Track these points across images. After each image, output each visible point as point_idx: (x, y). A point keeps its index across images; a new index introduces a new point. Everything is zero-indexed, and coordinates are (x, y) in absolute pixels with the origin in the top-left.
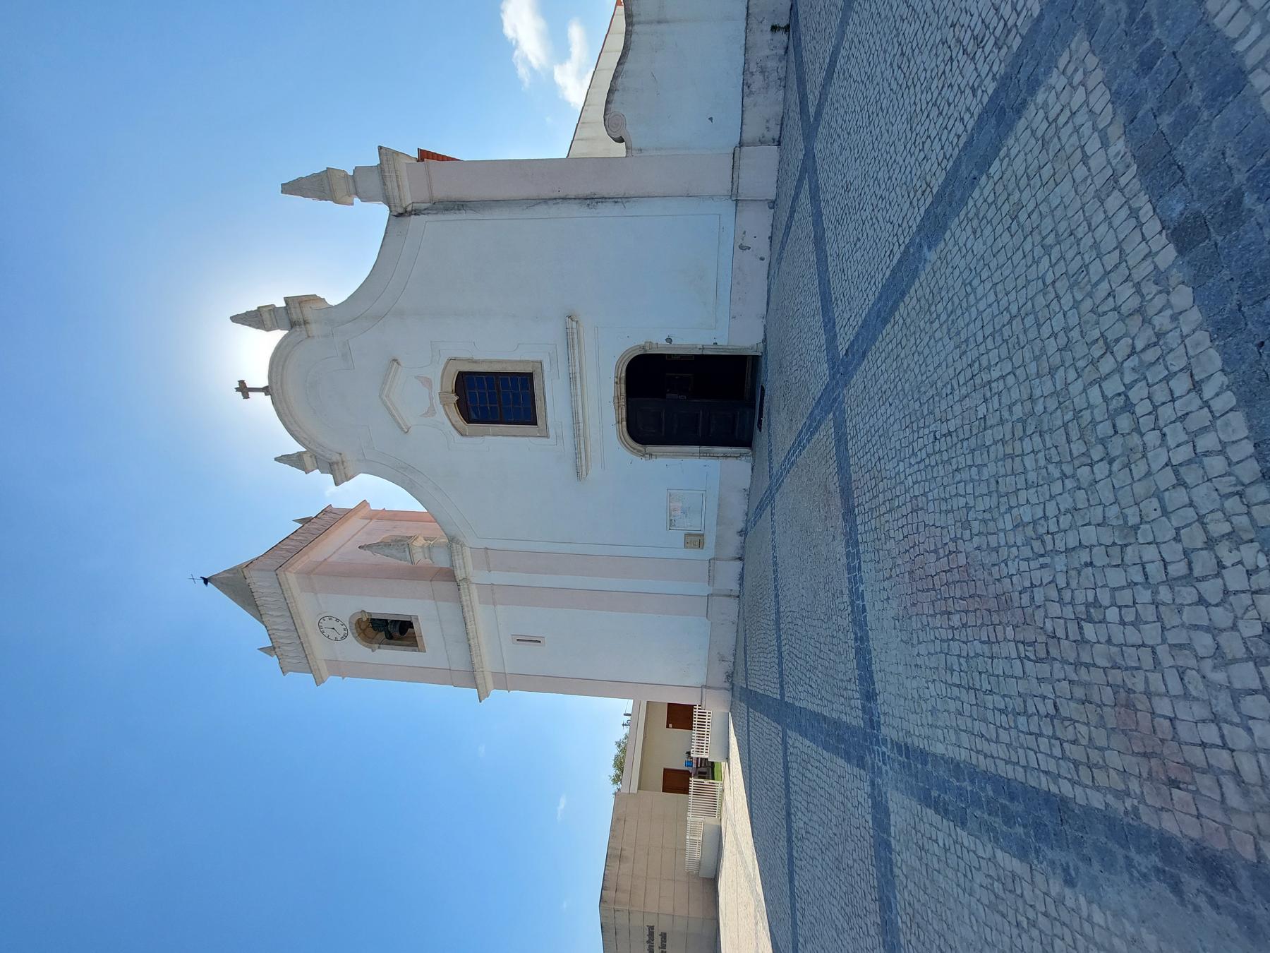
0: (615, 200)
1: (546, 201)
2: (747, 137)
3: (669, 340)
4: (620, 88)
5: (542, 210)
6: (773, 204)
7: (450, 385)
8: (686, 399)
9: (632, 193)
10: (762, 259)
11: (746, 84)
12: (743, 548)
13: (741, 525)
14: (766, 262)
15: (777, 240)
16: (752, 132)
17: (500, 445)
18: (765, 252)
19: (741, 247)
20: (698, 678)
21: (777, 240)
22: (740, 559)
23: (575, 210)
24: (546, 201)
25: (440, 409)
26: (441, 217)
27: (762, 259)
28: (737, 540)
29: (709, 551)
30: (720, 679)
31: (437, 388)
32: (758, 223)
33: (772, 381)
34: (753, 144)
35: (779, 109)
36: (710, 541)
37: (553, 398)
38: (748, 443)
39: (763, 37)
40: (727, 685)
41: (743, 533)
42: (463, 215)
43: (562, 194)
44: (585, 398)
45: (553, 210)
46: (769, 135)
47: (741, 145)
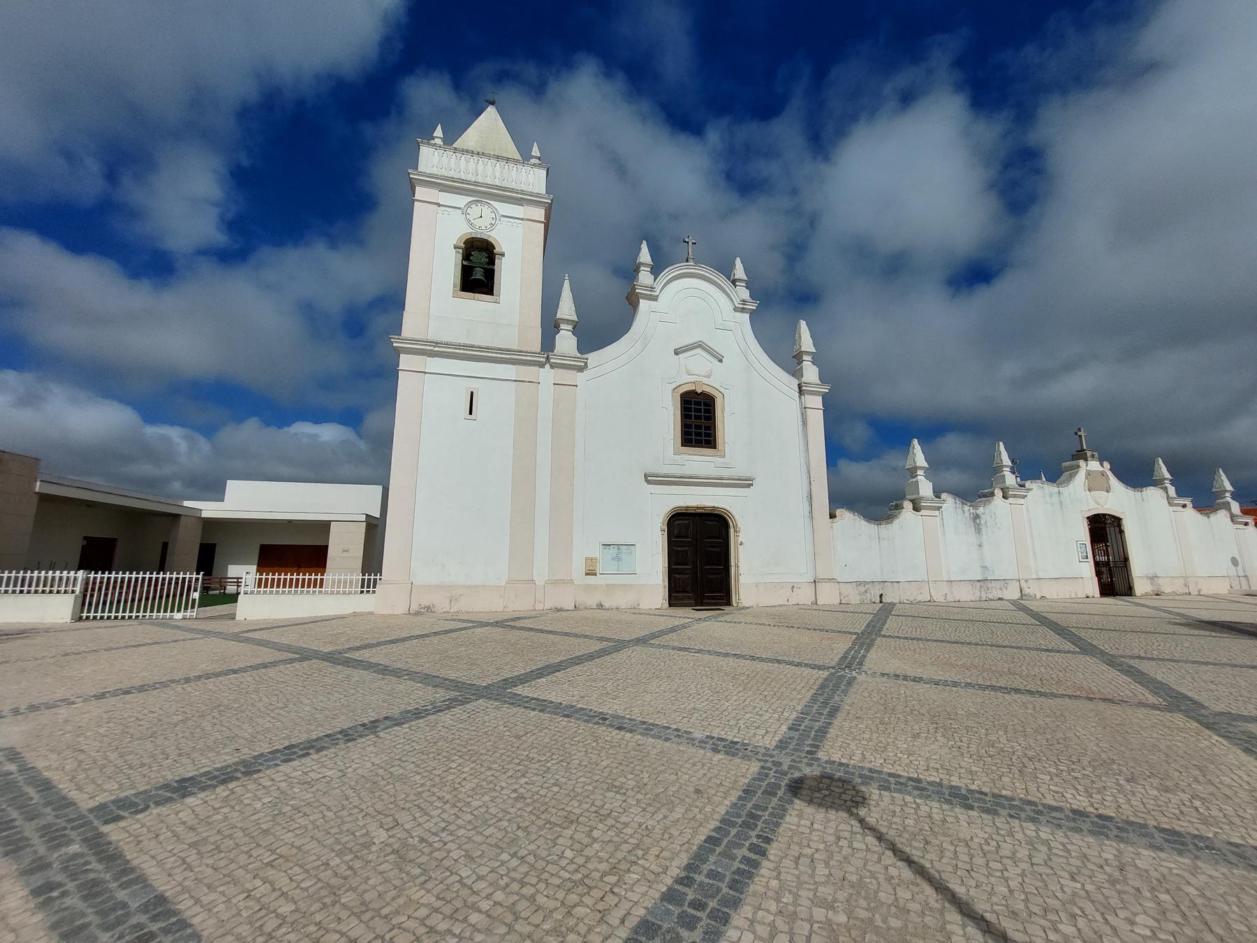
0: (811, 512)
5: (804, 468)
8: (700, 557)
11: (859, 583)
13: (607, 604)
17: (669, 420)
18: (792, 602)
20: (424, 575)
23: (806, 489)
25: (692, 379)
28: (592, 602)
30: (419, 601)
31: (705, 381)
32: (804, 596)
33: (727, 613)
36: (591, 580)
37: (698, 461)
39: (875, 593)
40: (414, 608)
41: (600, 606)
44: (701, 483)
45: (805, 476)
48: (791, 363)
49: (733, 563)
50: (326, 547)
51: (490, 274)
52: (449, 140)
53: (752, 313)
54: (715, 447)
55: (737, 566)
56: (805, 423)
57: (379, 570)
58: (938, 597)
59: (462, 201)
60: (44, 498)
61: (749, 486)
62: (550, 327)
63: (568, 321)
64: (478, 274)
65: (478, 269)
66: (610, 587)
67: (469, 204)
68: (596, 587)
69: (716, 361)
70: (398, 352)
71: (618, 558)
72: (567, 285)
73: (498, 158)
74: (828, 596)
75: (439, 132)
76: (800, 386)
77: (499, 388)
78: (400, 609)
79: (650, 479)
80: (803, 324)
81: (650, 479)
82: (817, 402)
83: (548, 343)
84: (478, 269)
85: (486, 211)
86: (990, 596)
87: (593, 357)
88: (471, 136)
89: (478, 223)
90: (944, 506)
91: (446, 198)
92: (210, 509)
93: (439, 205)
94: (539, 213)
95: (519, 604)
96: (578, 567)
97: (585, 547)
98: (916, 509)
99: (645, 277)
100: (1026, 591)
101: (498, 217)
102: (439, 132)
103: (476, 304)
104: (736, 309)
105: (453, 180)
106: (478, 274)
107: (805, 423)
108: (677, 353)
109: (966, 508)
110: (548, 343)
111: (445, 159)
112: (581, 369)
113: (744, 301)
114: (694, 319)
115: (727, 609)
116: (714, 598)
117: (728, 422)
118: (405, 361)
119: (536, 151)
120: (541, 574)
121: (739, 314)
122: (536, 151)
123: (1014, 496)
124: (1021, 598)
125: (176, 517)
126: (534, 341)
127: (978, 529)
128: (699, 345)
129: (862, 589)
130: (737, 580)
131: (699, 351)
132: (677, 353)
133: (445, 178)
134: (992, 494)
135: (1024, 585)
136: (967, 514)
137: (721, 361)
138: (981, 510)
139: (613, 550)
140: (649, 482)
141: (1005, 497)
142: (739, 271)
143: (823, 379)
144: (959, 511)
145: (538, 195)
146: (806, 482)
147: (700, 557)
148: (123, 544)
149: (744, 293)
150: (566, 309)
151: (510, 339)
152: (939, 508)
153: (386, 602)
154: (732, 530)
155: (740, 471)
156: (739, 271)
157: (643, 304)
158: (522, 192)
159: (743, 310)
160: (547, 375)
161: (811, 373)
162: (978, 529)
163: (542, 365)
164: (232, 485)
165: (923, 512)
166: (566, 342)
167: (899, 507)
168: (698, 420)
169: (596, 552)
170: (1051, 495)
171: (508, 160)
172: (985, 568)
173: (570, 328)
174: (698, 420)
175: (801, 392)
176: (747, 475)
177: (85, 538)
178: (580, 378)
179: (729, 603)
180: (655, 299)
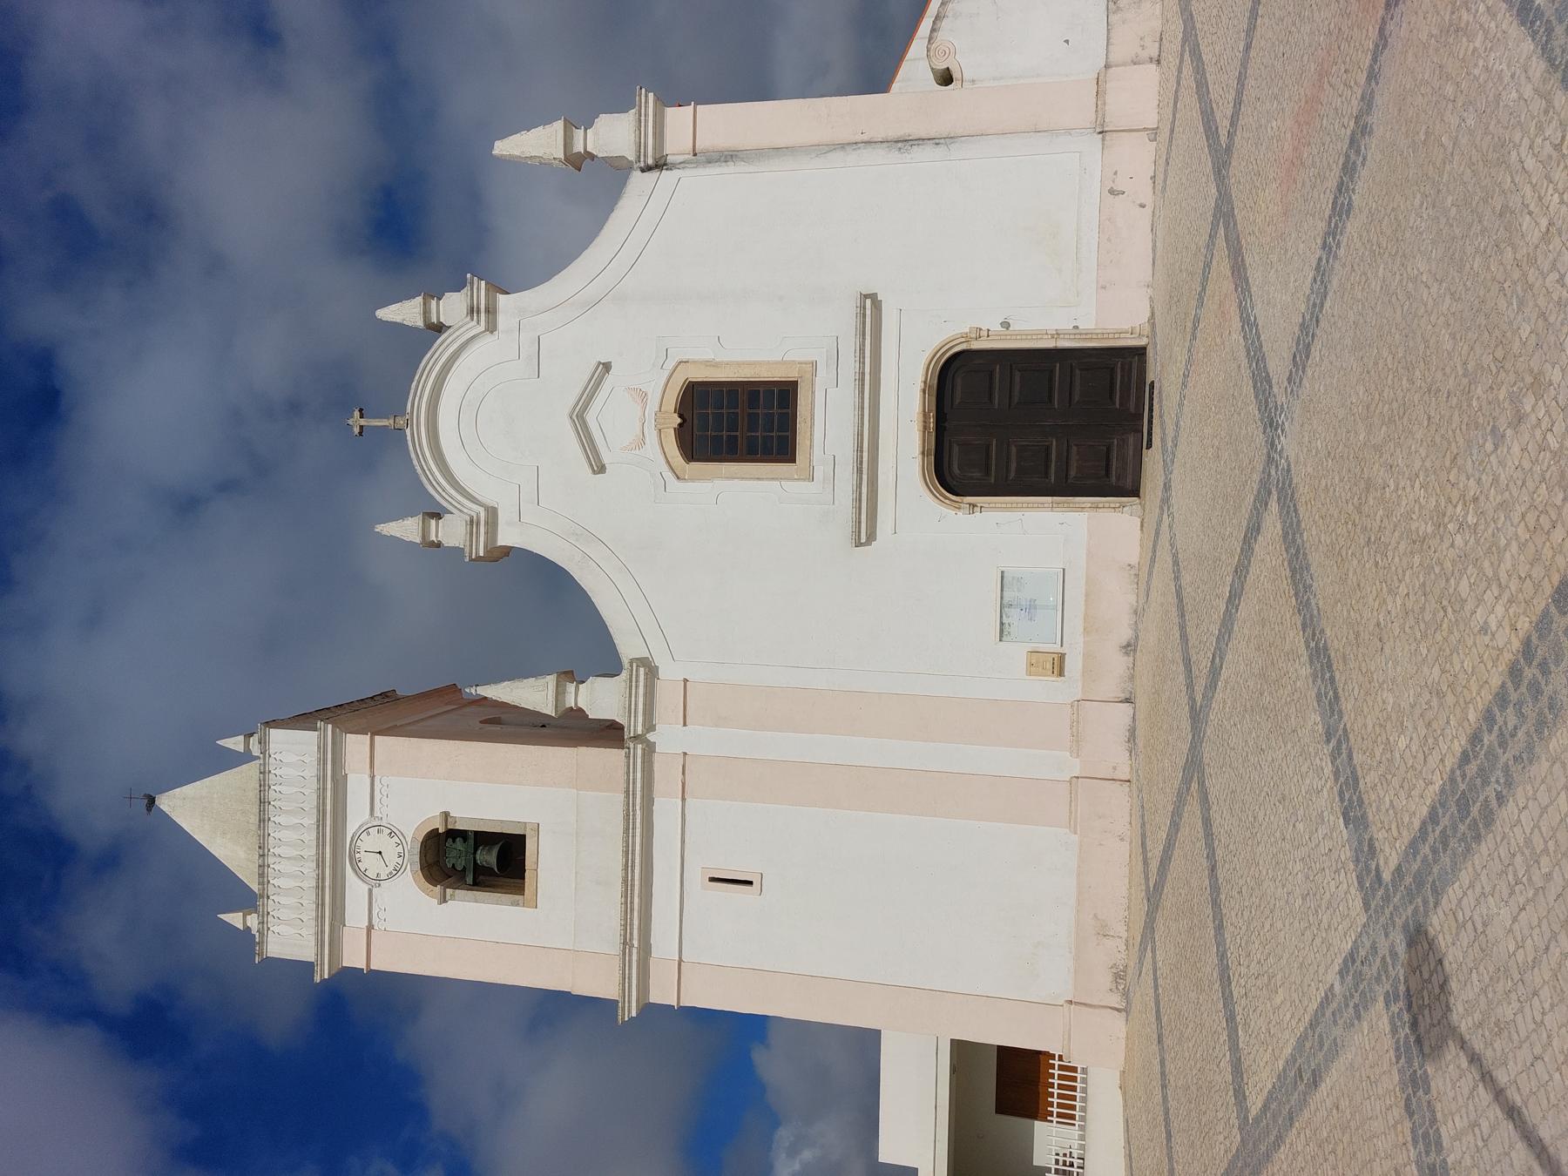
0: (935, 141)
1: (843, 146)
2: (1113, 58)
3: (1006, 325)
4: (950, 14)
5: (838, 156)
6: (1154, 133)
7: (671, 402)
8: (1032, 421)
9: (960, 132)
10: (1143, 206)
12: (1132, 678)
13: (1125, 634)
14: (1149, 210)
15: (1159, 180)
17: (739, 489)
18: (1146, 194)
19: (1112, 192)
20: (1056, 981)
21: (1159, 180)
22: (1127, 701)
24: (843, 146)
26: (700, 171)
27: (1143, 206)
28: (1120, 663)
30: (1101, 989)
31: (653, 405)
32: (1137, 160)
33: (1164, 372)
34: (1124, 64)
35: (1157, 24)
36: (1073, 665)
37: (826, 423)
38: (1134, 492)
40: (1116, 1000)
41: (1129, 648)
42: (730, 168)
43: (865, 138)
46: (1145, 55)
47: (1107, 66)
48: (596, 184)
49: (1050, 344)
50: (1000, 1048)
51: (483, 839)
52: (249, 900)
53: (498, 288)
54: (794, 384)
55: (1057, 335)
59: (355, 890)
61: (877, 305)
63: (560, 693)
64: (489, 858)
65: (480, 860)
66: (1091, 626)
67: (361, 874)
68: (1087, 656)
69: (609, 380)
70: (650, 1011)
71: (1031, 608)
73: (263, 821)
74: (1140, 95)
75: (235, 919)
76: (647, 169)
77: (701, 829)
79: (865, 532)
80: (503, 148)
81: (865, 532)
82: (678, 119)
83: (609, 733)
84: (480, 860)
87: (628, 648)
88: (231, 851)
91: (355, 915)
93: (370, 927)
94: (356, 744)
95: (1118, 806)
96: (1046, 689)
99: (451, 532)
102: (235, 919)
103: (543, 860)
104: (492, 328)
105: (320, 905)
108: (601, 469)
110: (609, 733)
111: (284, 914)
112: (652, 672)
113: (472, 311)
114: (524, 415)
115: (1150, 353)
117: (742, 352)
118: (663, 993)
119: (235, 743)
120: (1059, 764)
121: (502, 320)
122: (235, 743)
126: (609, 758)
128: (579, 418)
130: (1088, 335)
131: (590, 417)
132: (601, 469)
133: (320, 918)
137: (607, 367)
139: (1013, 616)
140: (871, 537)
142: (406, 312)
143: (621, 104)
145: (322, 748)
146: (867, 154)
147: (1032, 421)
149: (452, 307)
151: (607, 807)
154: (976, 345)
155: (843, 322)
156: (406, 312)
157: (505, 538)
158: (322, 779)
159: (491, 311)
160: (668, 738)
161: (612, 135)
163: (650, 748)
166: (600, 698)
168: (737, 422)
169: (1016, 653)
171: (263, 786)
173: (571, 687)
174: (737, 422)
175: (660, 165)
178: (669, 673)
179: (1140, 353)
180: (492, 513)
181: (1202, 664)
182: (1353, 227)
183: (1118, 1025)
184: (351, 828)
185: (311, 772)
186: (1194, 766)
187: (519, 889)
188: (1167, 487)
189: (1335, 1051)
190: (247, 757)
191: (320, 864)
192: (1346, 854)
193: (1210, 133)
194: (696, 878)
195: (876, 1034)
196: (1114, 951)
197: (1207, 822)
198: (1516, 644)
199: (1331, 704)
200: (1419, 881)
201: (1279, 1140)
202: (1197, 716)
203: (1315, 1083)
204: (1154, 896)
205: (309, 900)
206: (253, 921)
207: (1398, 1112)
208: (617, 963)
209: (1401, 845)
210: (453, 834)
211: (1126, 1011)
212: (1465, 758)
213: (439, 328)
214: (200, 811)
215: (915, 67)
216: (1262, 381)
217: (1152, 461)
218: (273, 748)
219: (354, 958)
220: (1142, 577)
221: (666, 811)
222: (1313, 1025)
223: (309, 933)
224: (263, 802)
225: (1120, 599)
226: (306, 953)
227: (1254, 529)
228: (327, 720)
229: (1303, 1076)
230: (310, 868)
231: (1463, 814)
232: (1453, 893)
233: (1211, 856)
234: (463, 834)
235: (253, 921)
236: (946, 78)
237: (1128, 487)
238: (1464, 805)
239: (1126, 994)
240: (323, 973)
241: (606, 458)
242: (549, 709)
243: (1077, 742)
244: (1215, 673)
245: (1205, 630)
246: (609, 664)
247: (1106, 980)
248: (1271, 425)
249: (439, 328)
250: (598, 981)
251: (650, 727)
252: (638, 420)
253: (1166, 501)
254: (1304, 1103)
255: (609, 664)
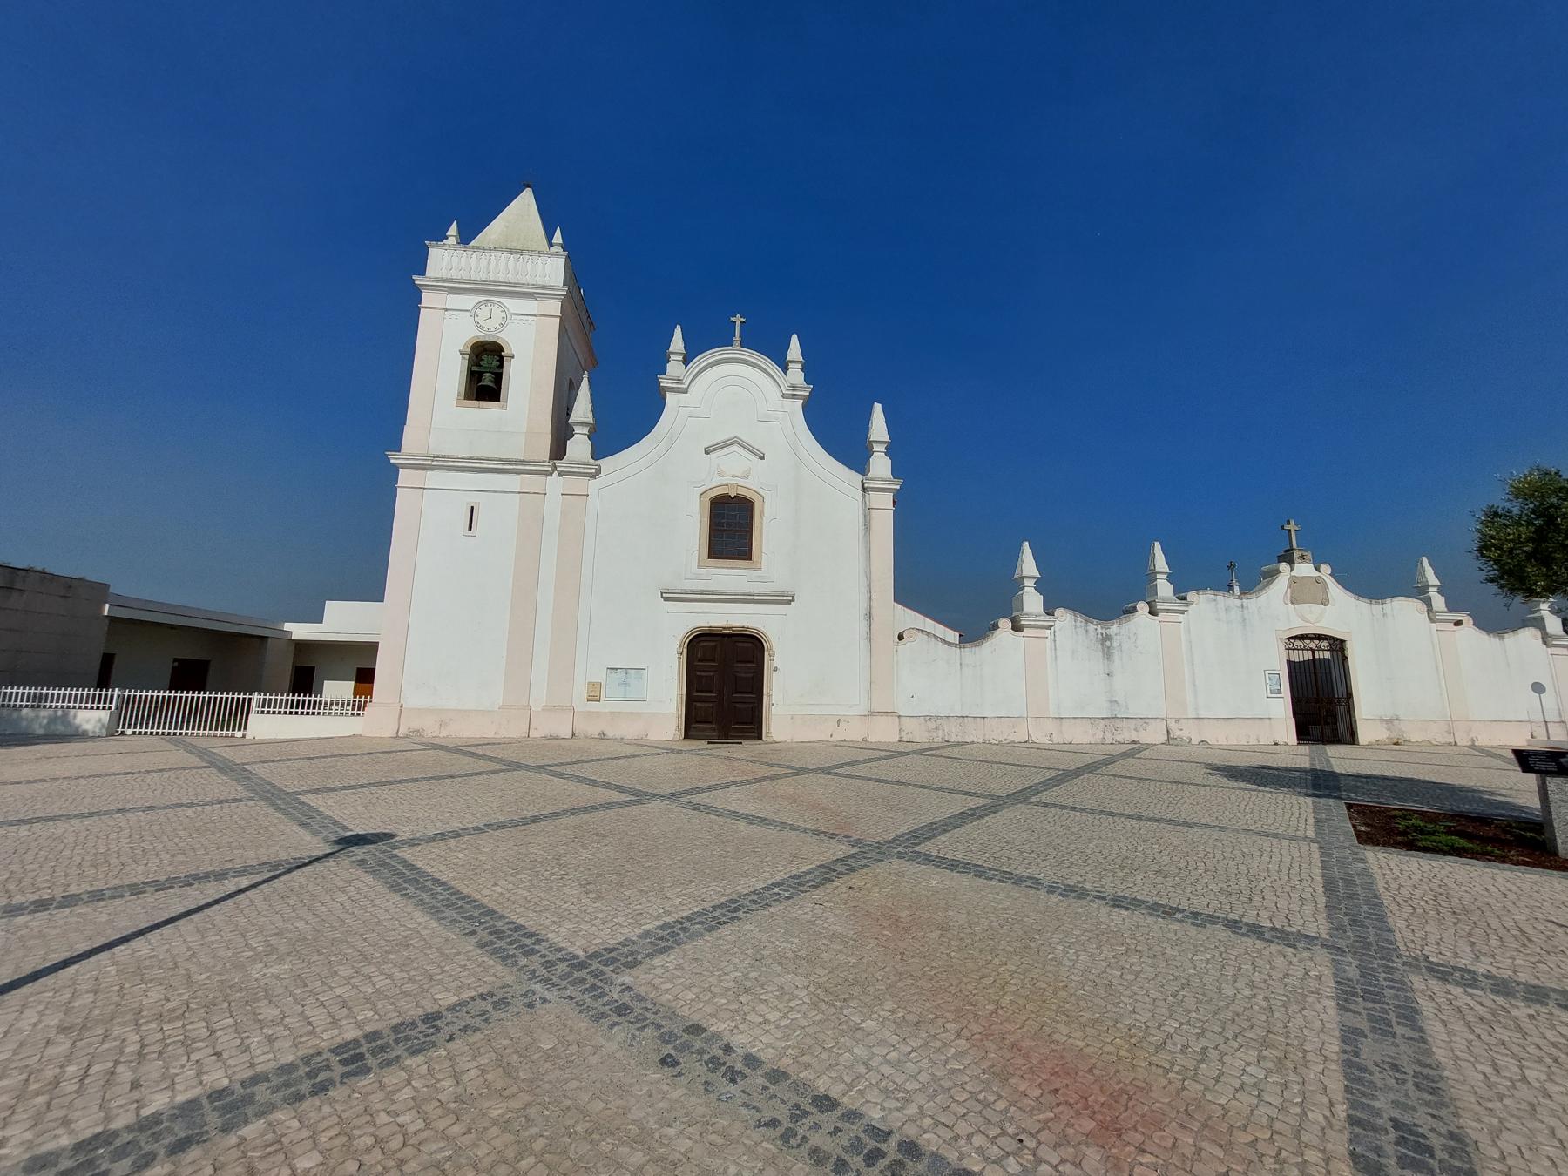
1: (869, 586)
6: (866, 740)
7: (742, 492)
8: (725, 683)
11: (930, 718)
13: (610, 734)
16: (907, 723)
17: (693, 527)
18: (836, 738)
20: (412, 700)
23: (864, 605)
24: (869, 586)
25: (725, 481)
28: (594, 730)
29: (581, 704)
30: (409, 724)
31: (742, 482)
32: (854, 733)
33: (748, 748)
36: (594, 705)
37: (729, 576)
41: (603, 736)
45: (864, 590)
51: (498, 378)
52: (465, 238)
55: (769, 696)
56: (867, 526)
57: (369, 693)
58: (1040, 738)
59: (469, 301)
60: (111, 619)
61: (789, 602)
62: (561, 434)
64: (487, 380)
65: (485, 375)
68: (599, 714)
69: (755, 459)
70: (395, 469)
71: (625, 684)
72: (585, 385)
73: (511, 251)
74: (884, 733)
75: (453, 230)
77: (500, 499)
78: (388, 732)
81: (668, 596)
82: (887, 500)
83: (558, 451)
84: (485, 375)
85: (497, 310)
86: (1120, 738)
87: (607, 463)
88: (495, 230)
89: (487, 324)
90: (1058, 624)
91: (455, 301)
92: (301, 631)
94: (555, 307)
95: (513, 729)
96: (580, 691)
97: (590, 670)
98: (1017, 628)
99: (675, 367)
100: (1176, 733)
101: (508, 316)
102: (453, 230)
103: (484, 412)
104: (784, 396)
106: (487, 380)
107: (867, 526)
109: (1092, 627)
110: (558, 451)
111: (455, 260)
112: (593, 476)
116: (742, 730)
117: (768, 531)
119: (558, 237)
123: (1167, 611)
124: (1167, 742)
125: (264, 638)
127: (1108, 654)
128: (734, 442)
129: (932, 725)
130: (769, 710)
131: (735, 447)
132: (707, 453)
134: (1134, 610)
135: (1172, 725)
136: (1092, 634)
137: (762, 458)
138: (1113, 630)
139: (620, 675)
140: (666, 599)
141: (1153, 612)
142: (795, 351)
143: (896, 473)
144: (1081, 631)
145: (552, 288)
147: (725, 683)
148: (208, 665)
149: (796, 375)
150: (582, 410)
151: (514, 450)
152: (1050, 627)
153: (374, 723)
156: (795, 351)
158: (534, 286)
160: (555, 484)
161: (880, 465)
162: (1108, 654)
164: (330, 606)
165: (1027, 632)
166: (579, 446)
167: (995, 627)
168: (730, 527)
169: (600, 676)
170: (1227, 610)
171: (532, 252)
172: (1113, 702)
173: (586, 430)
174: (730, 527)
175: (864, 490)
176: (789, 590)
177: (175, 660)
179: (760, 738)
180: (685, 391)
181: (568, 770)
182: (742, 825)
183: (390, 733)
184: (505, 301)
185: (540, 281)
186: (516, 766)
187: (468, 397)
188: (680, 751)
189: (315, 833)
190: (551, 245)
191: (484, 282)
192: (418, 835)
193: (841, 765)
194: (473, 499)
195: (380, 598)
196: (431, 730)
197: (481, 773)
198: (478, 897)
199: (503, 826)
200: (385, 865)
201: (278, 809)
202: (541, 768)
203: (302, 824)
204: (456, 750)
205: (464, 275)
206: (452, 241)
207: (265, 859)
208: (423, 452)
209: (408, 857)
210: (501, 360)
211: (397, 737)
212: (435, 880)
213: (785, 369)
214: (523, 211)
215: (909, 618)
216: (687, 793)
217: (702, 744)
218: (554, 259)
219: (428, 298)
220: (640, 743)
221: (513, 482)
222: (335, 823)
223: (444, 274)
224: (522, 252)
225: (627, 730)
226: (430, 272)
227: (621, 789)
228: (569, 291)
229: (307, 818)
230: (482, 276)
231: (408, 881)
232: (368, 878)
233: (460, 776)
234: (501, 366)
235: (452, 241)
236: (901, 637)
237: (688, 734)
238: (410, 881)
239: (407, 737)
240: (418, 280)
241: (712, 455)
242: (572, 418)
243: (548, 709)
244: (560, 775)
245: (587, 772)
246: (599, 452)
247: (415, 725)
248: (674, 796)
249: (785, 369)
250: (412, 439)
251: (561, 474)
252: (733, 473)
253: (673, 751)
254: (294, 819)
255: (599, 452)
